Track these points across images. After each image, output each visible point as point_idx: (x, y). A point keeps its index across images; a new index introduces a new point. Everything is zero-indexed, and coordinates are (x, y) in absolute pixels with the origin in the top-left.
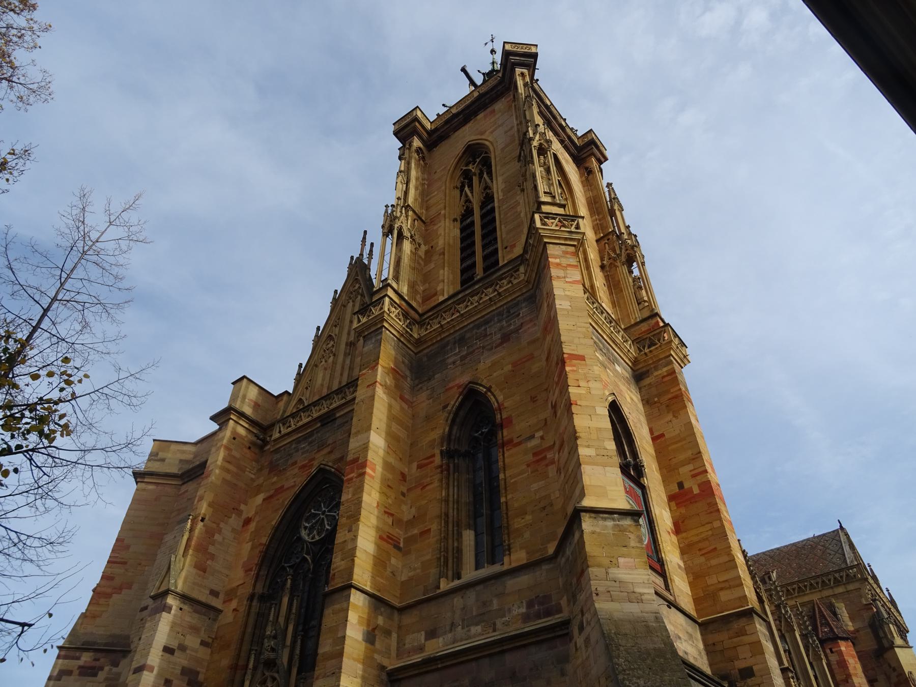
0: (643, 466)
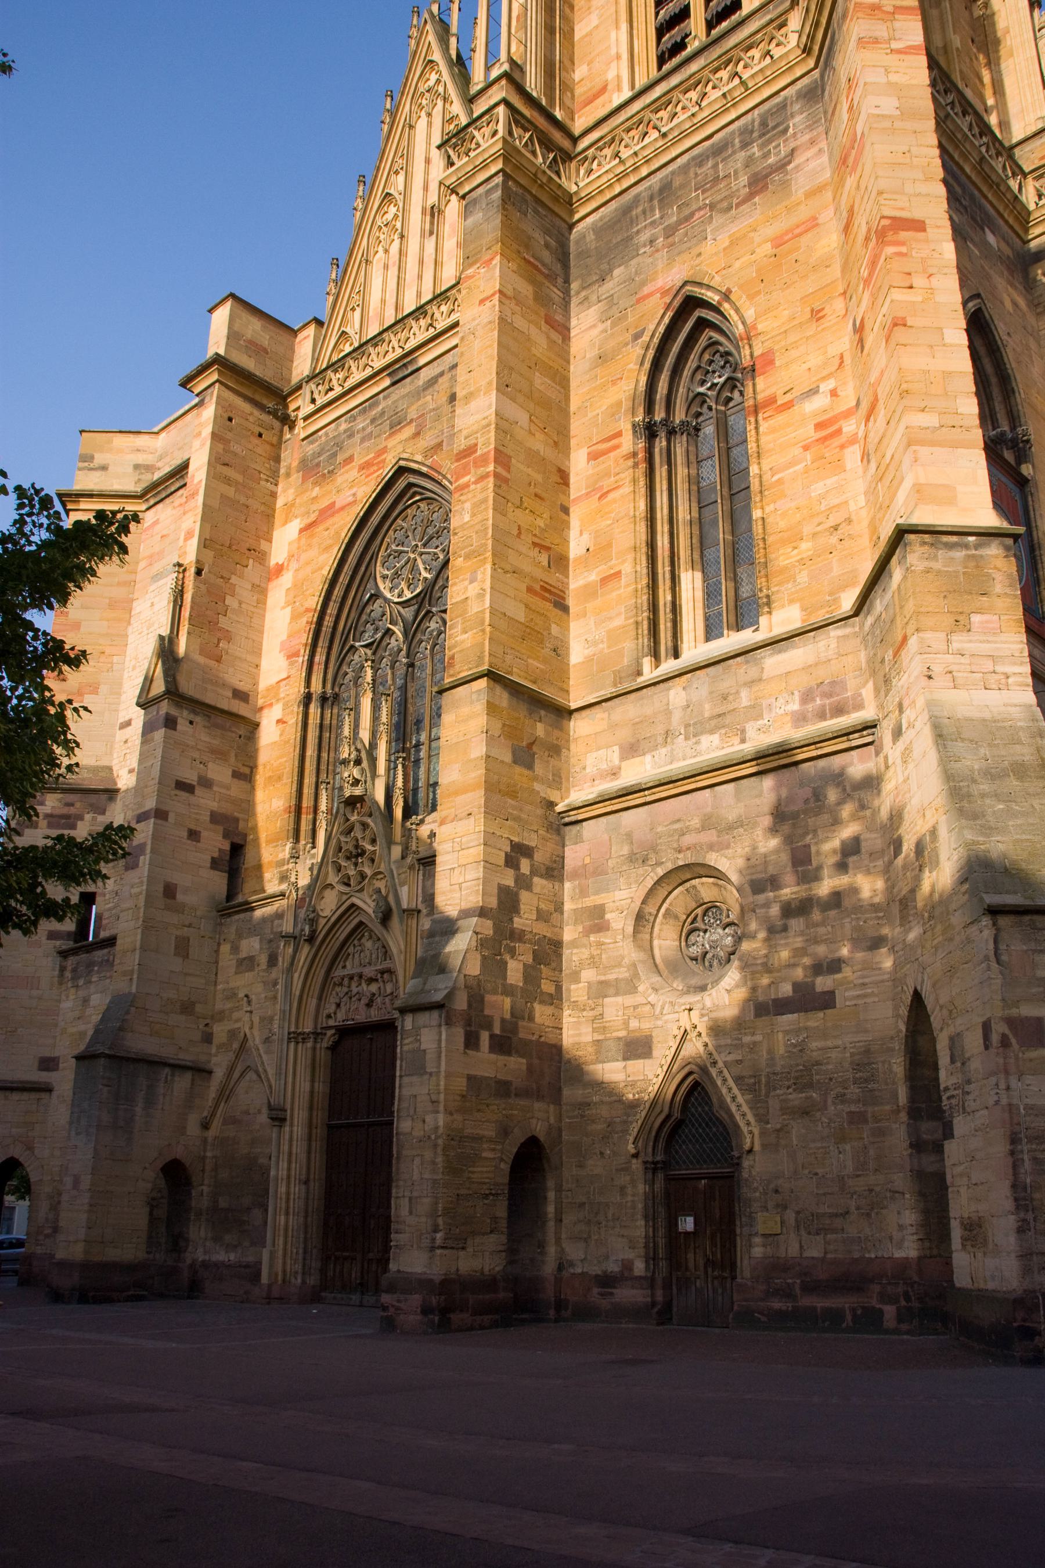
0: (1028, 441)
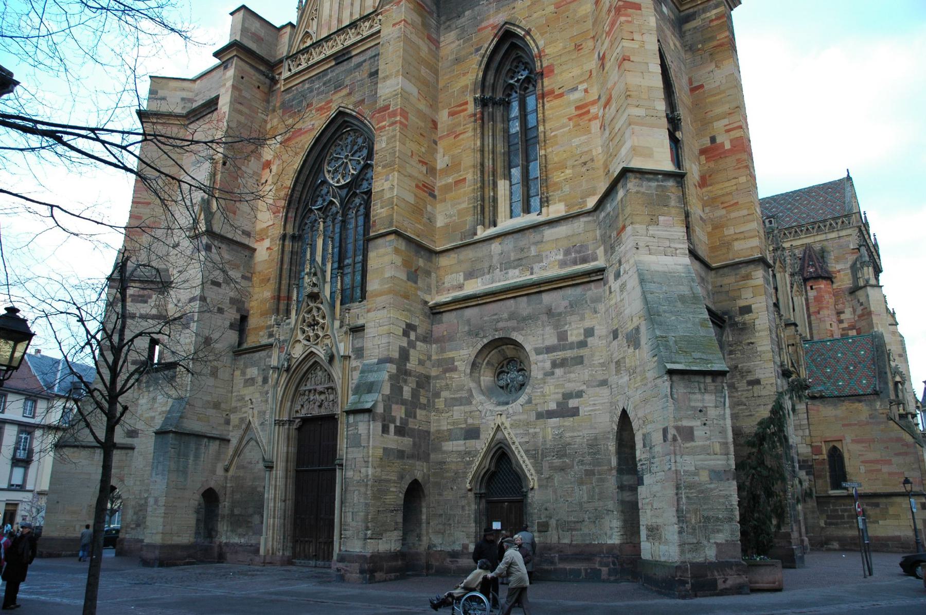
0: (680, 119)
